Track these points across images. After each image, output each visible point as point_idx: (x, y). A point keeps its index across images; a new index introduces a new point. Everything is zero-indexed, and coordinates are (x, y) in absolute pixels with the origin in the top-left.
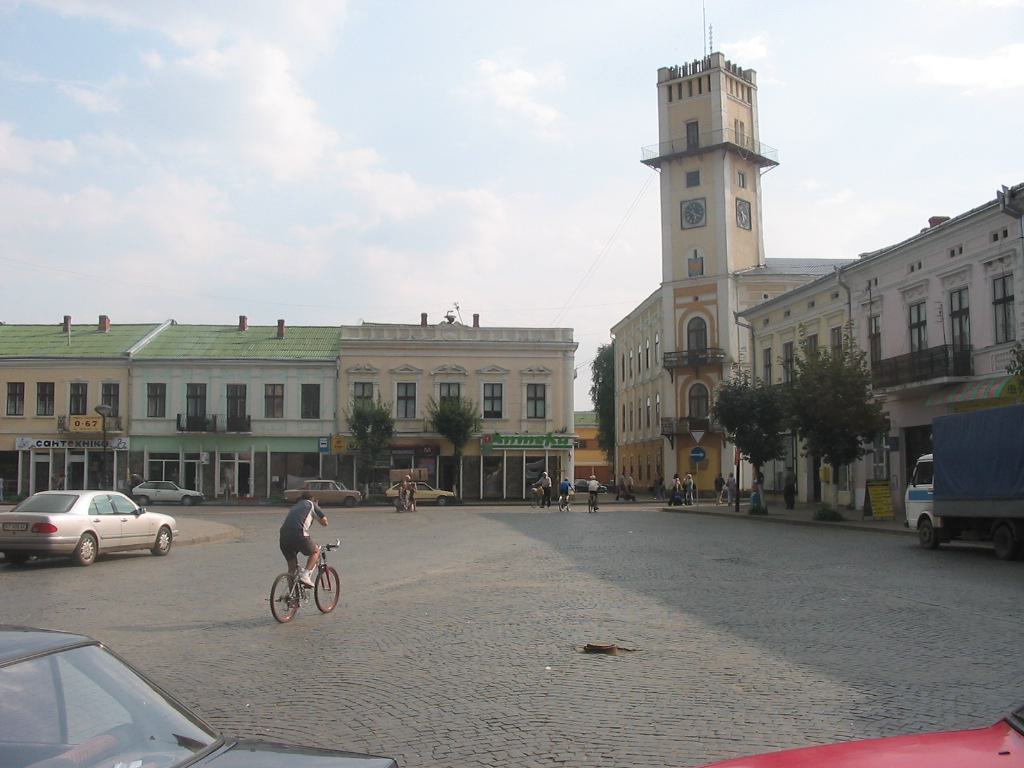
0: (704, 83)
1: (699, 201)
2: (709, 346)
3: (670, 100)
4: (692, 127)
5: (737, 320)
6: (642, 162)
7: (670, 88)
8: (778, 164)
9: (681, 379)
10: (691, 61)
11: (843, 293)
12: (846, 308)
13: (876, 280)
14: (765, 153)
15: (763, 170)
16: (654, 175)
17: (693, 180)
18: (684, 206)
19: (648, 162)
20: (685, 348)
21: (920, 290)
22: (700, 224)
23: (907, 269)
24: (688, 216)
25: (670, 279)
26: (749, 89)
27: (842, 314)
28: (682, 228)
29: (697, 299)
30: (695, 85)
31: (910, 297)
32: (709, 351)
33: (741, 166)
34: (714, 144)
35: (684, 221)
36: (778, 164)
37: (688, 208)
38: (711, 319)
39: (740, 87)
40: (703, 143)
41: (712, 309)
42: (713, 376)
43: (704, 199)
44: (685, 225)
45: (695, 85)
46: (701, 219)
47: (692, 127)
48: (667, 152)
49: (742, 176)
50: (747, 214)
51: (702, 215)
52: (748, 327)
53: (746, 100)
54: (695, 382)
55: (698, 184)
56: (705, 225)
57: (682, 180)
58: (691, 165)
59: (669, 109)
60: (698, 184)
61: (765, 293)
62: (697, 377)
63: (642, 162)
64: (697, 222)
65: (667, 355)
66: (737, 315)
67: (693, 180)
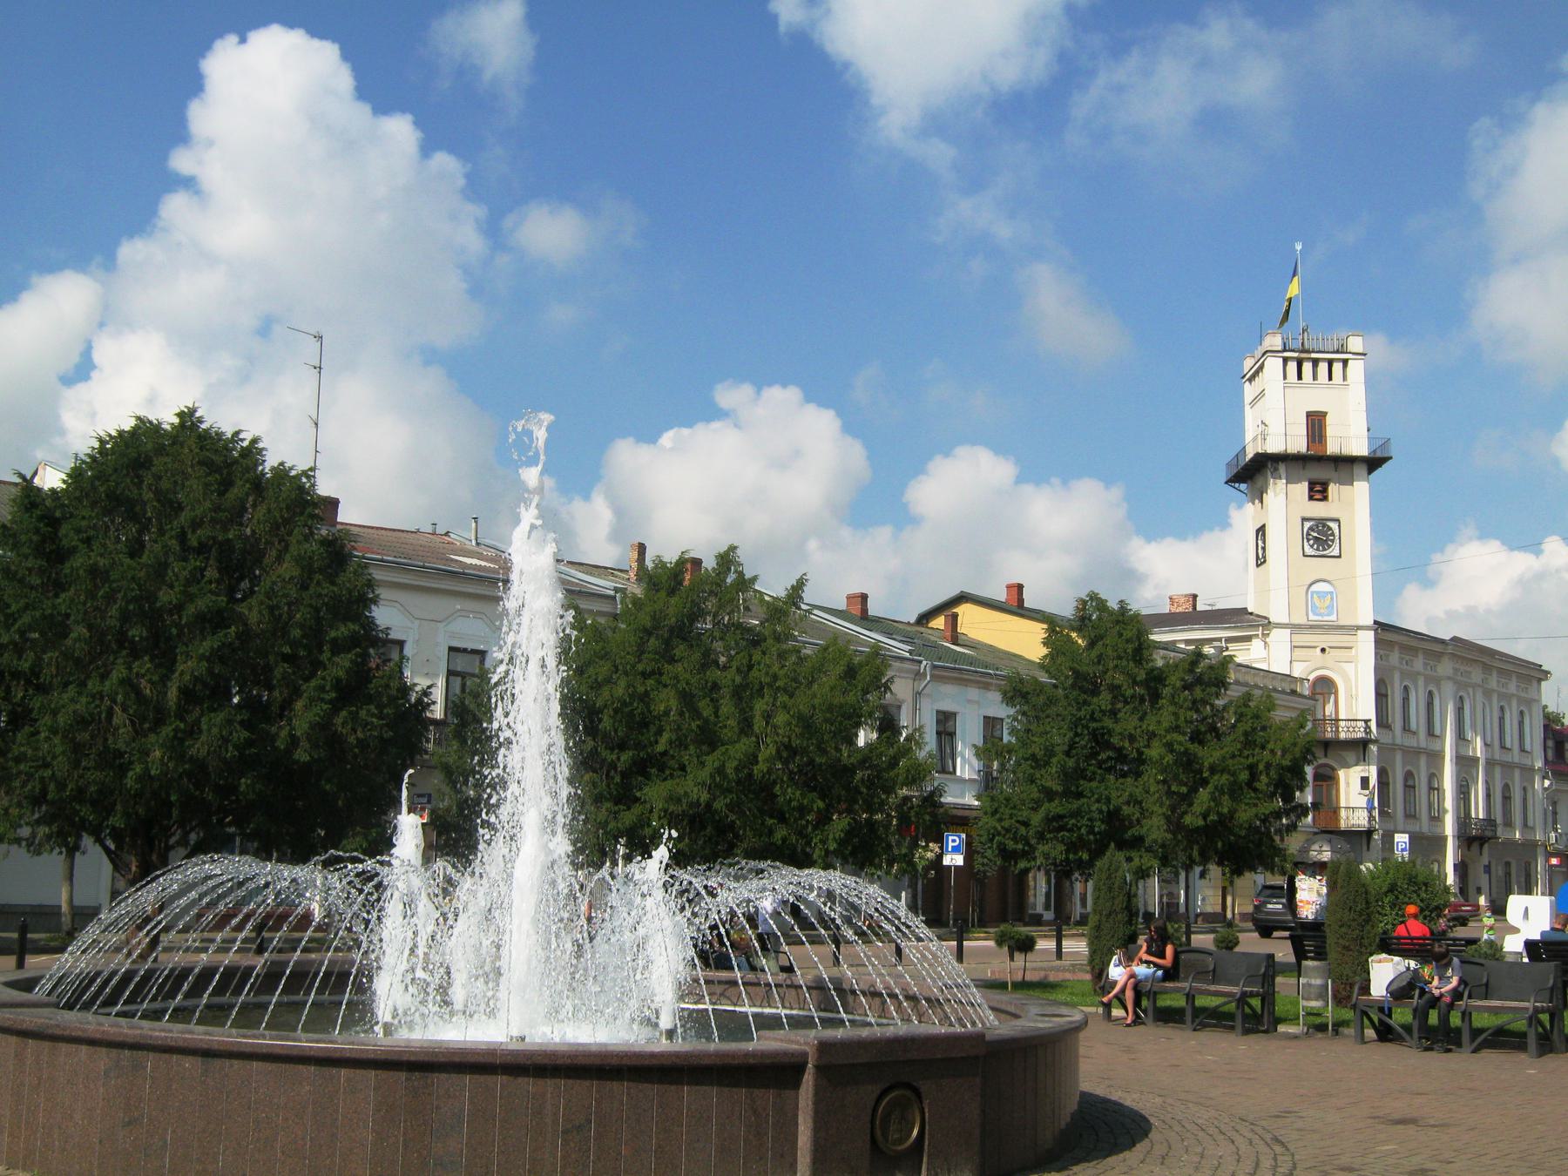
0: (1337, 367)
1: (1331, 524)
4: (1316, 423)
7: (1285, 360)
17: (1318, 491)
18: (1307, 525)
29: (1323, 650)
30: (1323, 367)
32: (1342, 724)
37: (1311, 529)
42: (1350, 756)
43: (1338, 520)
44: (1309, 551)
45: (1323, 367)
47: (1316, 423)
55: (1325, 498)
57: (1303, 487)
58: (1318, 473)
60: (1325, 498)
67: (1318, 491)
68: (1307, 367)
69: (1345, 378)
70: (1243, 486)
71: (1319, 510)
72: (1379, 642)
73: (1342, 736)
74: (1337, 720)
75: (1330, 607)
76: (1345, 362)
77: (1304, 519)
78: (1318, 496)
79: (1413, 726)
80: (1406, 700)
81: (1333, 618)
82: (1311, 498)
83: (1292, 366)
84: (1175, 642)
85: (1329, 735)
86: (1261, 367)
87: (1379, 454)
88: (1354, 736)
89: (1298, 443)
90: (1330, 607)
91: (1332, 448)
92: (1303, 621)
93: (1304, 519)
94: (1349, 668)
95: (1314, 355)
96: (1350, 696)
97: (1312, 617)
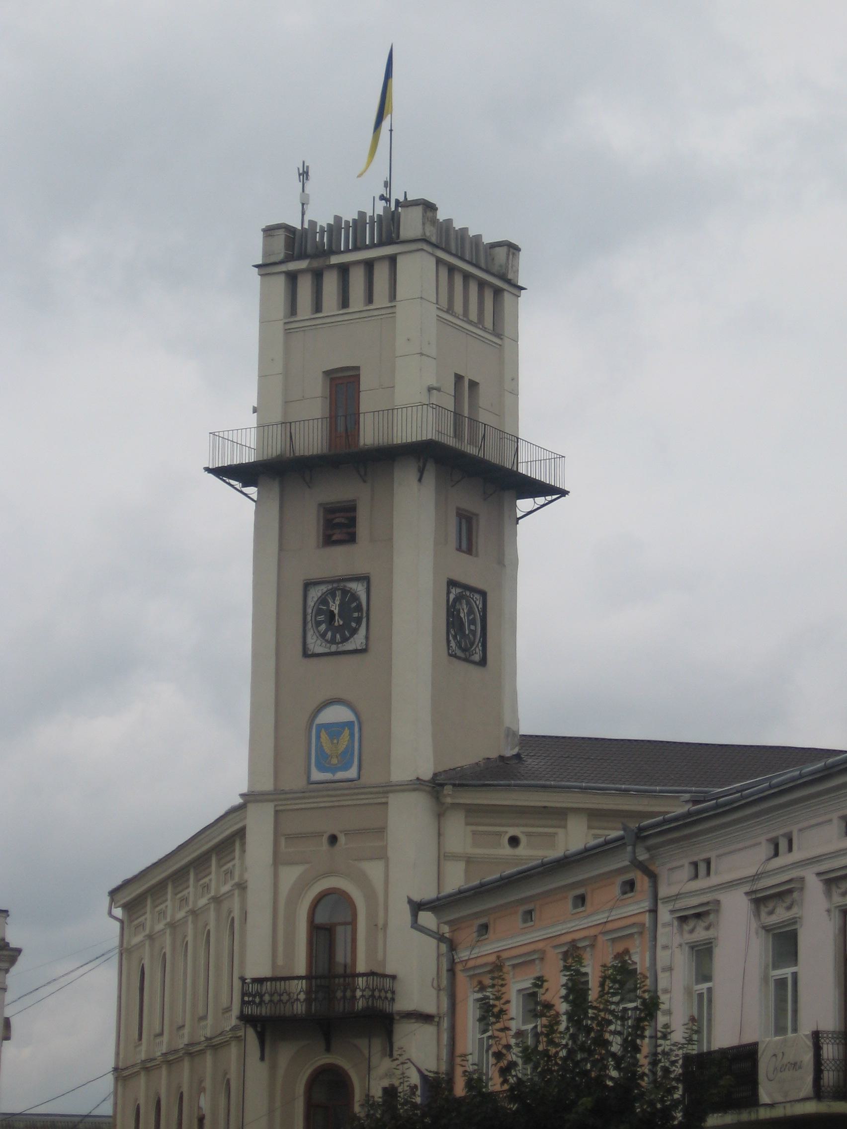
0: (381, 273)
1: (353, 586)
2: (361, 968)
5: (415, 916)
6: (208, 470)
7: (292, 278)
8: (563, 493)
9: (285, 1053)
10: (349, 215)
11: (643, 883)
12: (647, 919)
13: (708, 862)
14: (528, 465)
15: (524, 505)
16: (239, 507)
17: (339, 527)
18: (315, 594)
19: (222, 472)
20: (301, 968)
21: (788, 901)
22: (349, 646)
23: (765, 850)
24: (323, 618)
25: (267, 785)
26: (498, 292)
27: (641, 933)
28: (307, 654)
29: (333, 839)
31: (771, 913)
32: (361, 982)
33: (466, 498)
34: (397, 440)
36: (563, 493)
37: (323, 600)
39: (473, 288)
40: (370, 435)
41: (374, 870)
43: (365, 579)
44: (316, 645)
45: (357, 278)
46: (354, 632)
48: (275, 449)
49: (467, 520)
50: (472, 626)
51: (359, 621)
52: (441, 938)
53: (488, 323)
54: (325, 1059)
55: (351, 539)
58: (336, 490)
59: (288, 332)
60: (351, 539)
61: (512, 831)
62: (328, 1049)
63: (208, 470)
64: (345, 640)
65: (253, 990)
66: (417, 907)
67: (339, 527)
68: (331, 284)
69: (393, 296)
71: (339, 561)
73: (360, 1004)
75: (349, 750)
76: (392, 260)
81: (352, 773)
90: (349, 750)
92: (301, 783)
93: (308, 585)
94: (374, 870)
95: (335, 260)
97: (317, 775)
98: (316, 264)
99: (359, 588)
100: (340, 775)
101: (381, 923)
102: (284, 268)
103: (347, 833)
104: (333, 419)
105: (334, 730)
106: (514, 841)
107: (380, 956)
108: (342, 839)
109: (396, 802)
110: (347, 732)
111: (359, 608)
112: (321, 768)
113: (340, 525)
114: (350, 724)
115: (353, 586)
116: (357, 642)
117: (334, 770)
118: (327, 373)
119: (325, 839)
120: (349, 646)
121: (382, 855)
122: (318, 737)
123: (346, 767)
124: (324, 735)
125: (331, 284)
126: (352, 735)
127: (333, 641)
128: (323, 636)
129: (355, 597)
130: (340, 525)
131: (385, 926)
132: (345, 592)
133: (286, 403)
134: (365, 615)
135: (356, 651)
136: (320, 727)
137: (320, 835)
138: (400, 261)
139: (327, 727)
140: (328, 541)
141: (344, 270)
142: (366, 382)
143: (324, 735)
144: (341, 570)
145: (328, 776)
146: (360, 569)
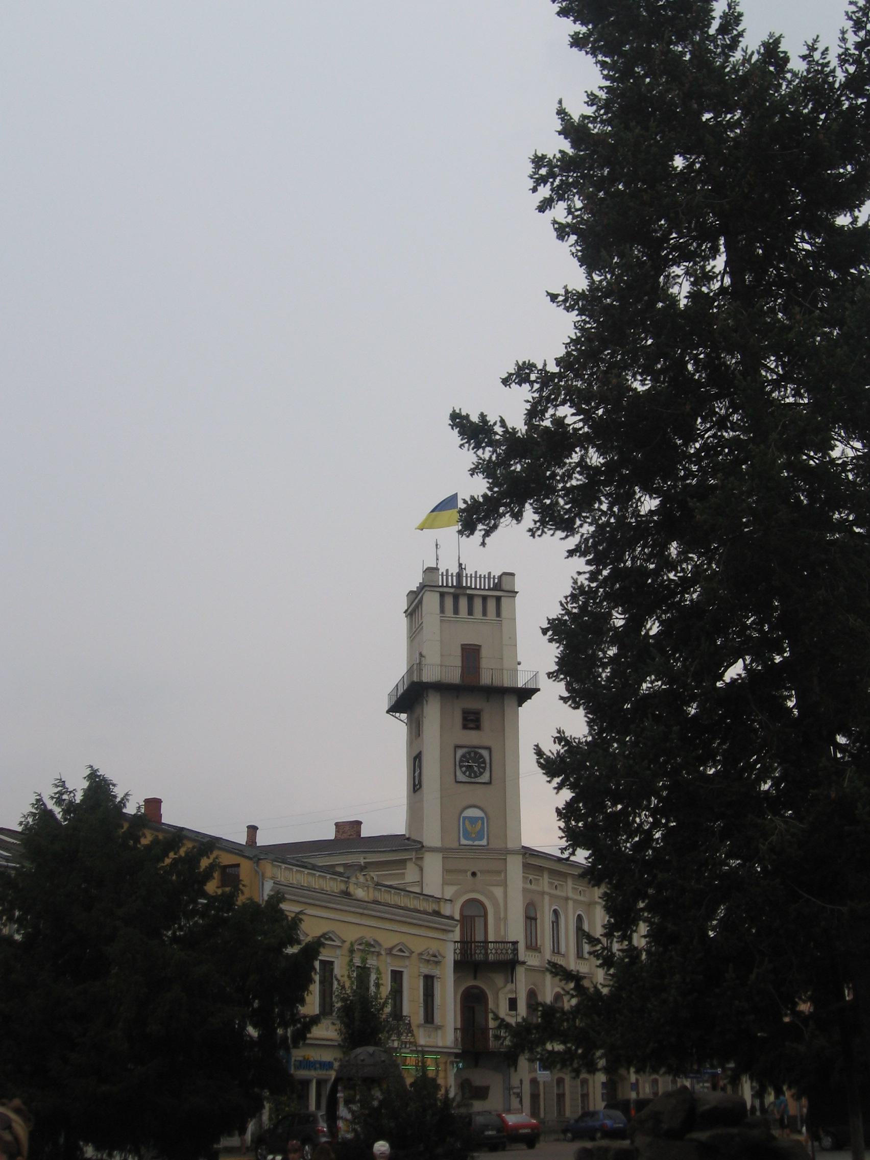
0: (491, 605)
3: (442, 610)
4: (471, 654)
7: (442, 595)
17: (472, 721)
18: (460, 752)
22: (477, 780)
29: (474, 874)
32: (491, 946)
35: (459, 773)
37: (463, 756)
38: (496, 904)
41: (498, 892)
42: (499, 979)
43: (489, 749)
44: (461, 777)
45: (478, 603)
46: (481, 774)
47: (471, 654)
54: (471, 983)
55: (478, 727)
56: (490, 783)
58: (472, 704)
59: (441, 621)
62: (475, 978)
67: (472, 721)
68: (463, 603)
69: (498, 614)
70: (404, 716)
71: (472, 738)
72: (526, 866)
73: (491, 957)
74: (486, 942)
76: (498, 599)
77: (457, 747)
78: (471, 725)
79: (563, 950)
80: (556, 923)
81: (484, 842)
82: (465, 727)
83: (449, 602)
84: (333, 866)
85: (479, 957)
86: (420, 602)
87: (530, 686)
88: (502, 957)
89: (454, 676)
91: (486, 679)
92: (455, 845)
94: (498, 892)
95: (469, 592)
96: (498, 919)
97: (464, 842)
98: (459, 591)
99: (485, 753)
100: (476, 843)
101: (502, 916)
102: (441, 590)
103: (481, 872)
104: (464, 668)
105: (473, 820)
106: (531, 882)
107: (502, 933)
108: (479, 874)
109: (510, 859)
110: (480, 822)
111: (484, 762)
112: (466, 838)
113: (472, 721)
114: (482, 819)
115: (480, 751)
116: (485, 778)
117: (474, 840)
118: (462, 645)
119: (469, 873)
120: (477, 780)
121: (504, 884)
122: (464, 823)
123: (481, 839)
124: (467, 822)
125: (463, 603)
126: (483, 823)
127: (470, 776)
128: (464, 773)
129: (481, 756)
130: (472, 721)
131: (506, 918)
132: (476, 753)
133: (442, 655)
134: (488, 766)
135: (484, 783)
136: (465, 818)
137: (465, 871)
138: (503, 599)
139: (470, 818)
140: (465, 727)
141: (471, 598)
142: (484, 653)
143: (467, 822)
144: (475, 742)
145: (470, 843)
146: (486, 743)
